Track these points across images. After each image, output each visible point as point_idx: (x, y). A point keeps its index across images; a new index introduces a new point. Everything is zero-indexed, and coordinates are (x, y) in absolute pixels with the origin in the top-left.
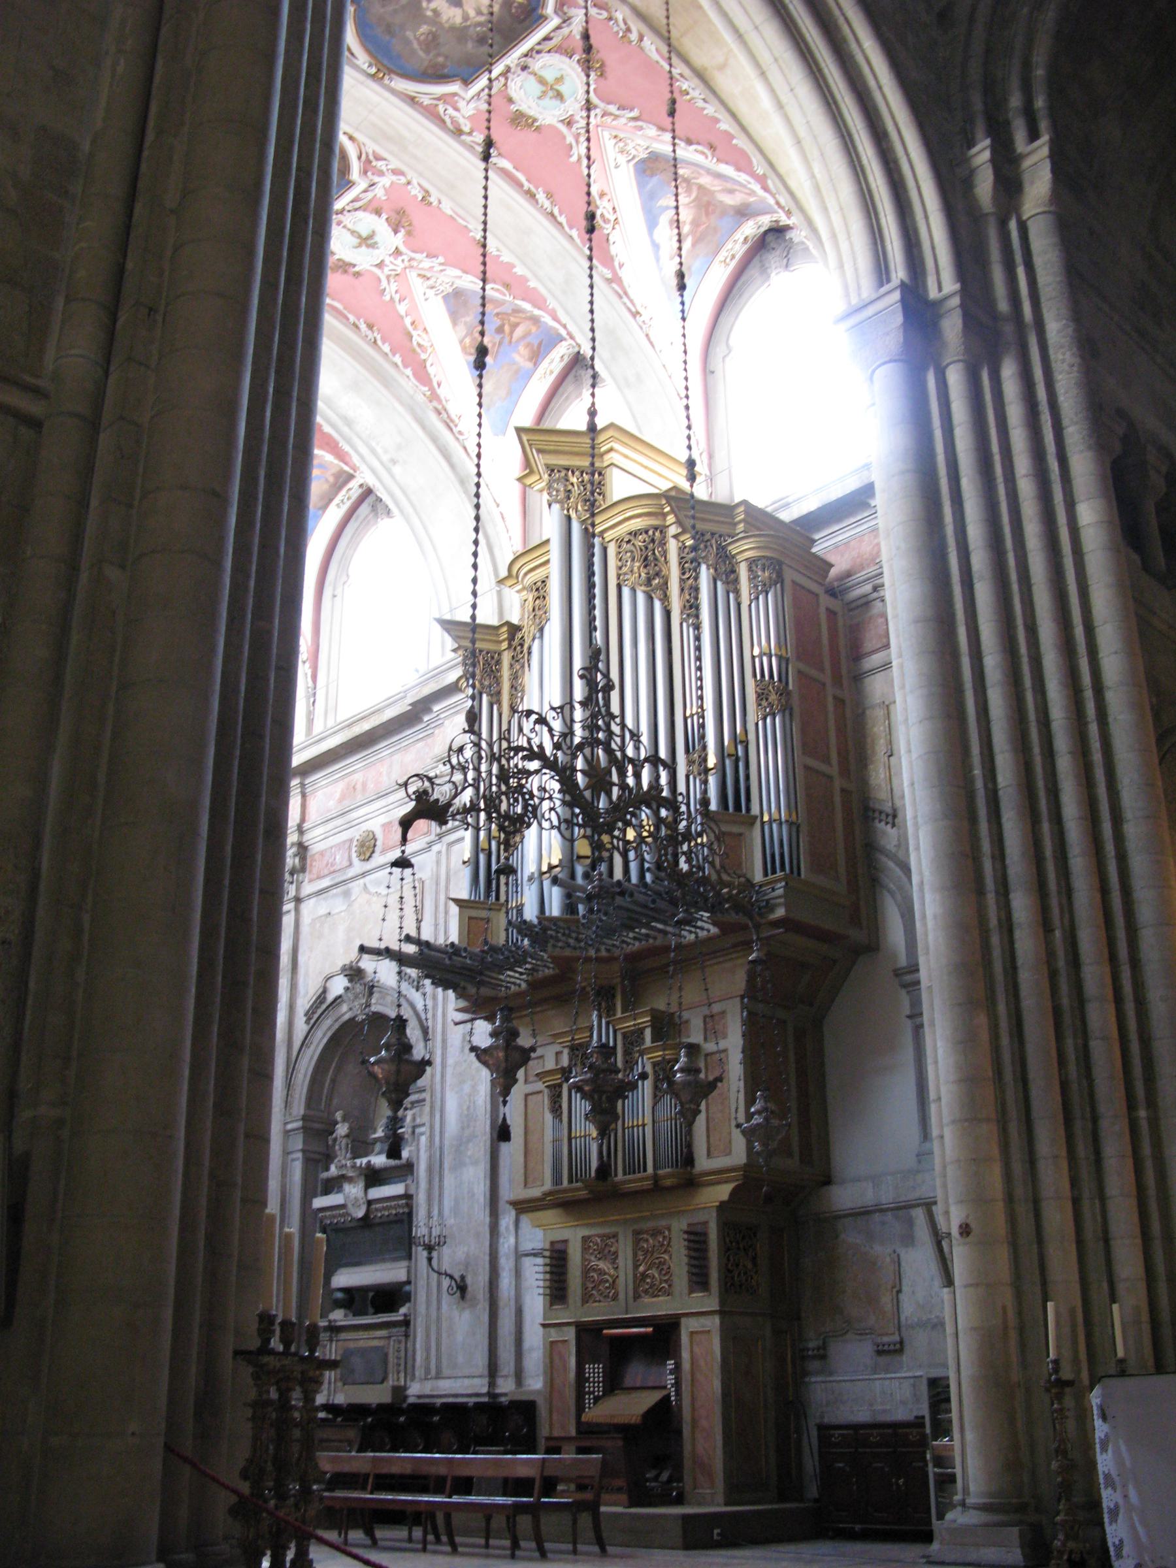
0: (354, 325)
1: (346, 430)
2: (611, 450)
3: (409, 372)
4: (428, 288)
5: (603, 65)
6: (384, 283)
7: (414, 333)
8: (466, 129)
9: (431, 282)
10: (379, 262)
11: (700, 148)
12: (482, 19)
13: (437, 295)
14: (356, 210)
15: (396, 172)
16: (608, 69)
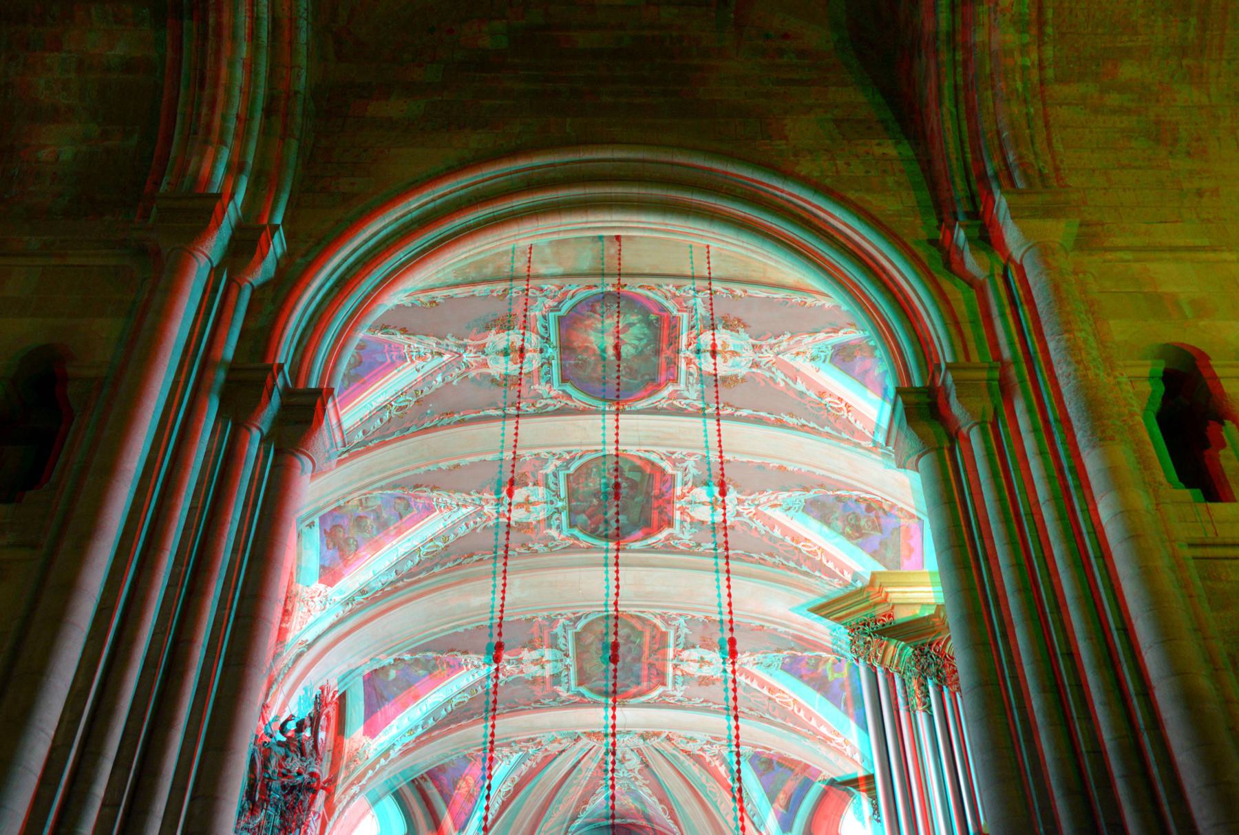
0: (760, 558)
1: (812, 632)
2: (887, 593)
3: (817, 573)
4: (786, 510)
5: (739, 321)
6: (754, 526)
7: (799, 546)
9: (784, 506)
10: (735, 513)
11: (845, 330)
12: (645, 341)
13: (797, 511)
15: (690, 455)
16: (745, 319)
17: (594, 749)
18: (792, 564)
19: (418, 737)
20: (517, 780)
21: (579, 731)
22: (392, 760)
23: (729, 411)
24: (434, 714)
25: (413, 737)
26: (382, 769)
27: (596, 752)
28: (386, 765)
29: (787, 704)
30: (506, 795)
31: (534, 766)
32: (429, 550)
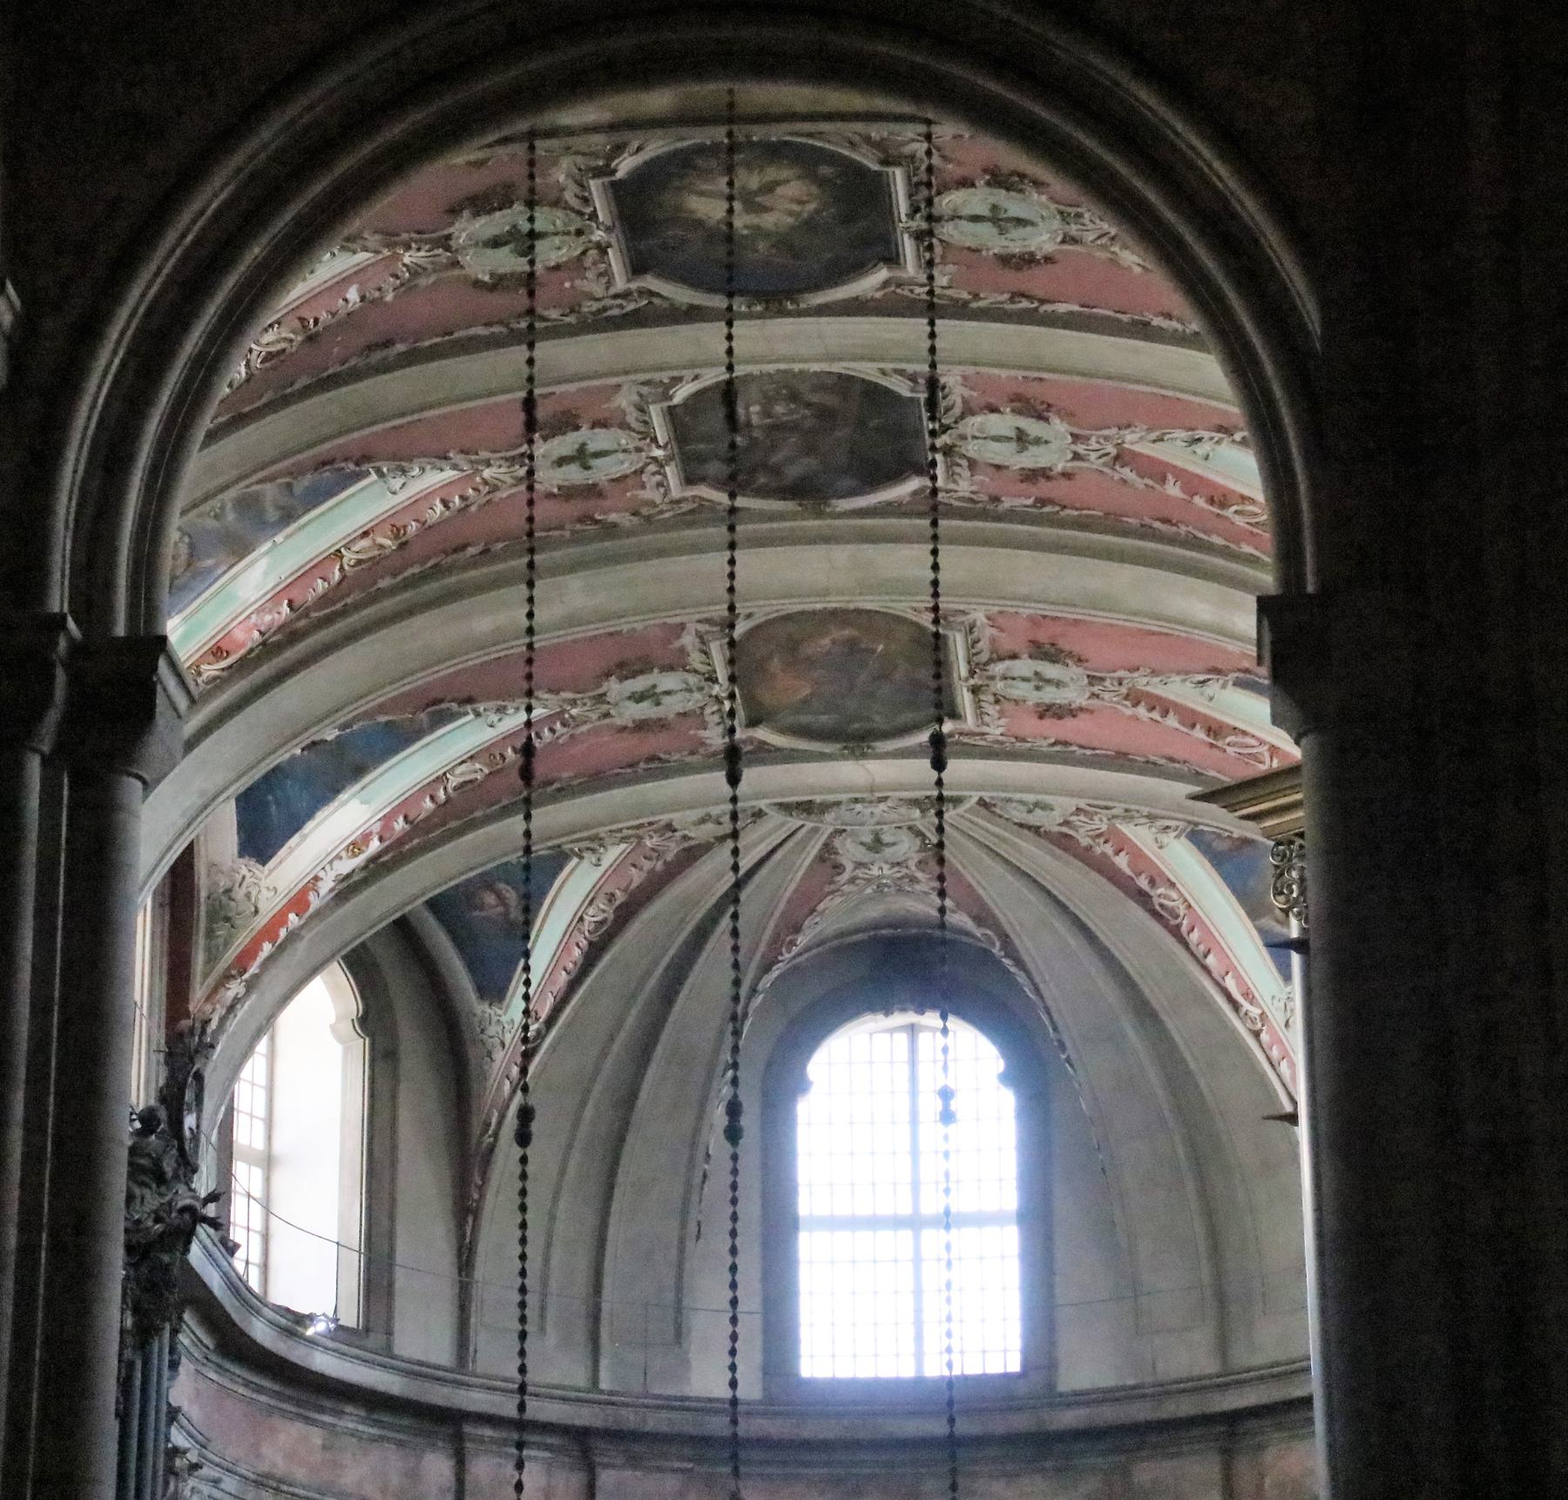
8: (965, 296)
10: (1070, 456)
14: (962, 417)
17: (804, 831)
18: (1217, 540)
19: (373, 859)
20: (620, 897)
21: (762, 804)
22: (319, 914)
23: (1025, 304)
24: (404, 807)
25: (360, 860)
26: (293, 936)
27: (803, 845)
28: (302, 927)
29: (1255, 757)
30: (596, 929)
31: (659, 866)
32: (360, 557)
